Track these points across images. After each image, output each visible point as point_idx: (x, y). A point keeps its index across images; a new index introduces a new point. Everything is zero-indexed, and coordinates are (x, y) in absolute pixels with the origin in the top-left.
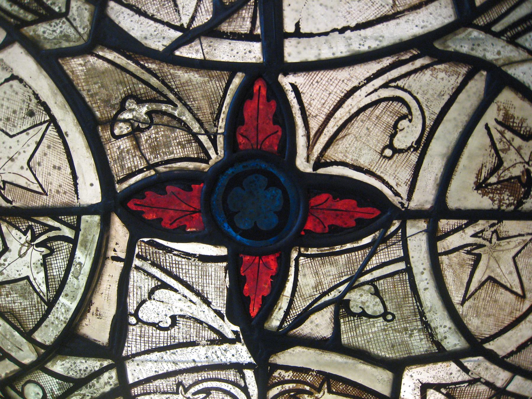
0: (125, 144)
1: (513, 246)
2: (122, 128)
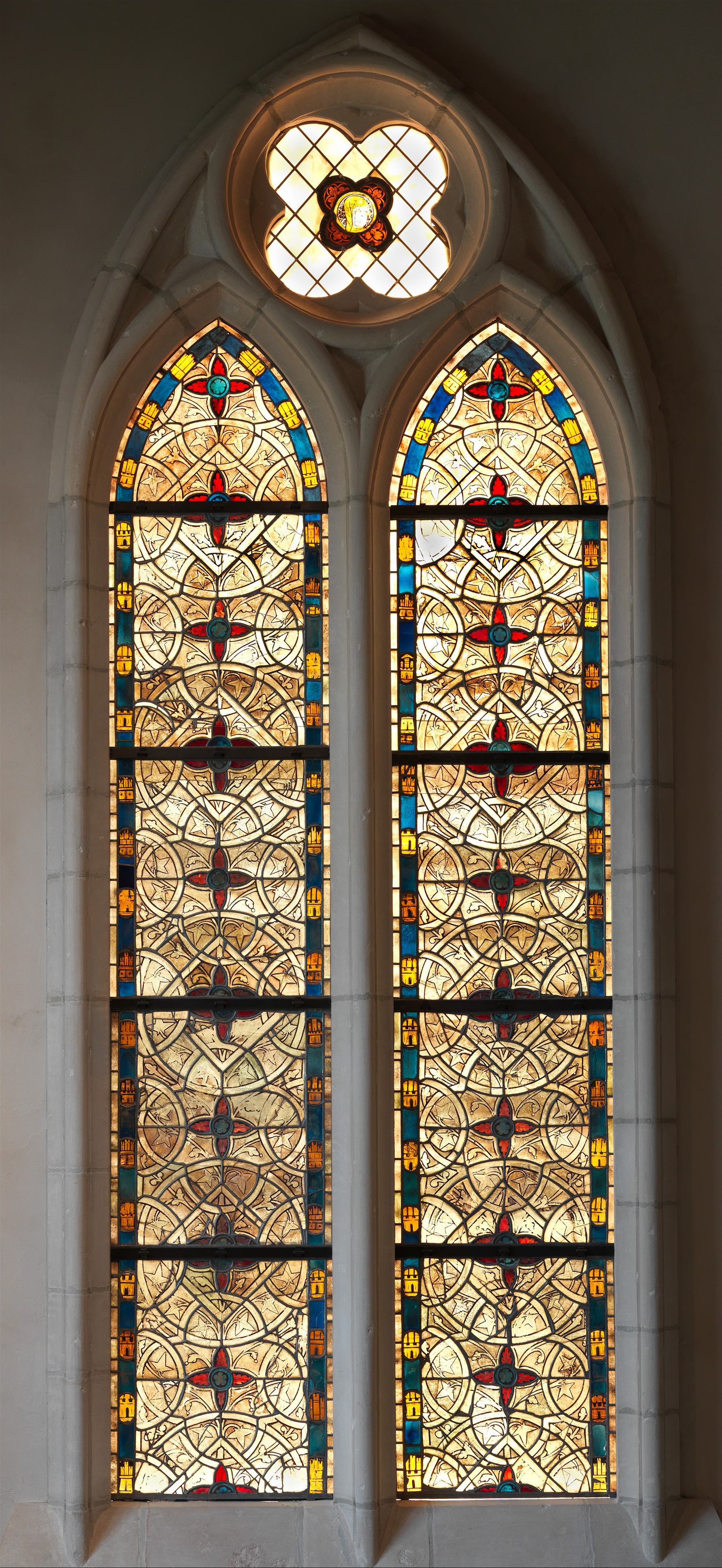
0: (475, 1362)
1: (569, 1386)
2: (474, 1358)
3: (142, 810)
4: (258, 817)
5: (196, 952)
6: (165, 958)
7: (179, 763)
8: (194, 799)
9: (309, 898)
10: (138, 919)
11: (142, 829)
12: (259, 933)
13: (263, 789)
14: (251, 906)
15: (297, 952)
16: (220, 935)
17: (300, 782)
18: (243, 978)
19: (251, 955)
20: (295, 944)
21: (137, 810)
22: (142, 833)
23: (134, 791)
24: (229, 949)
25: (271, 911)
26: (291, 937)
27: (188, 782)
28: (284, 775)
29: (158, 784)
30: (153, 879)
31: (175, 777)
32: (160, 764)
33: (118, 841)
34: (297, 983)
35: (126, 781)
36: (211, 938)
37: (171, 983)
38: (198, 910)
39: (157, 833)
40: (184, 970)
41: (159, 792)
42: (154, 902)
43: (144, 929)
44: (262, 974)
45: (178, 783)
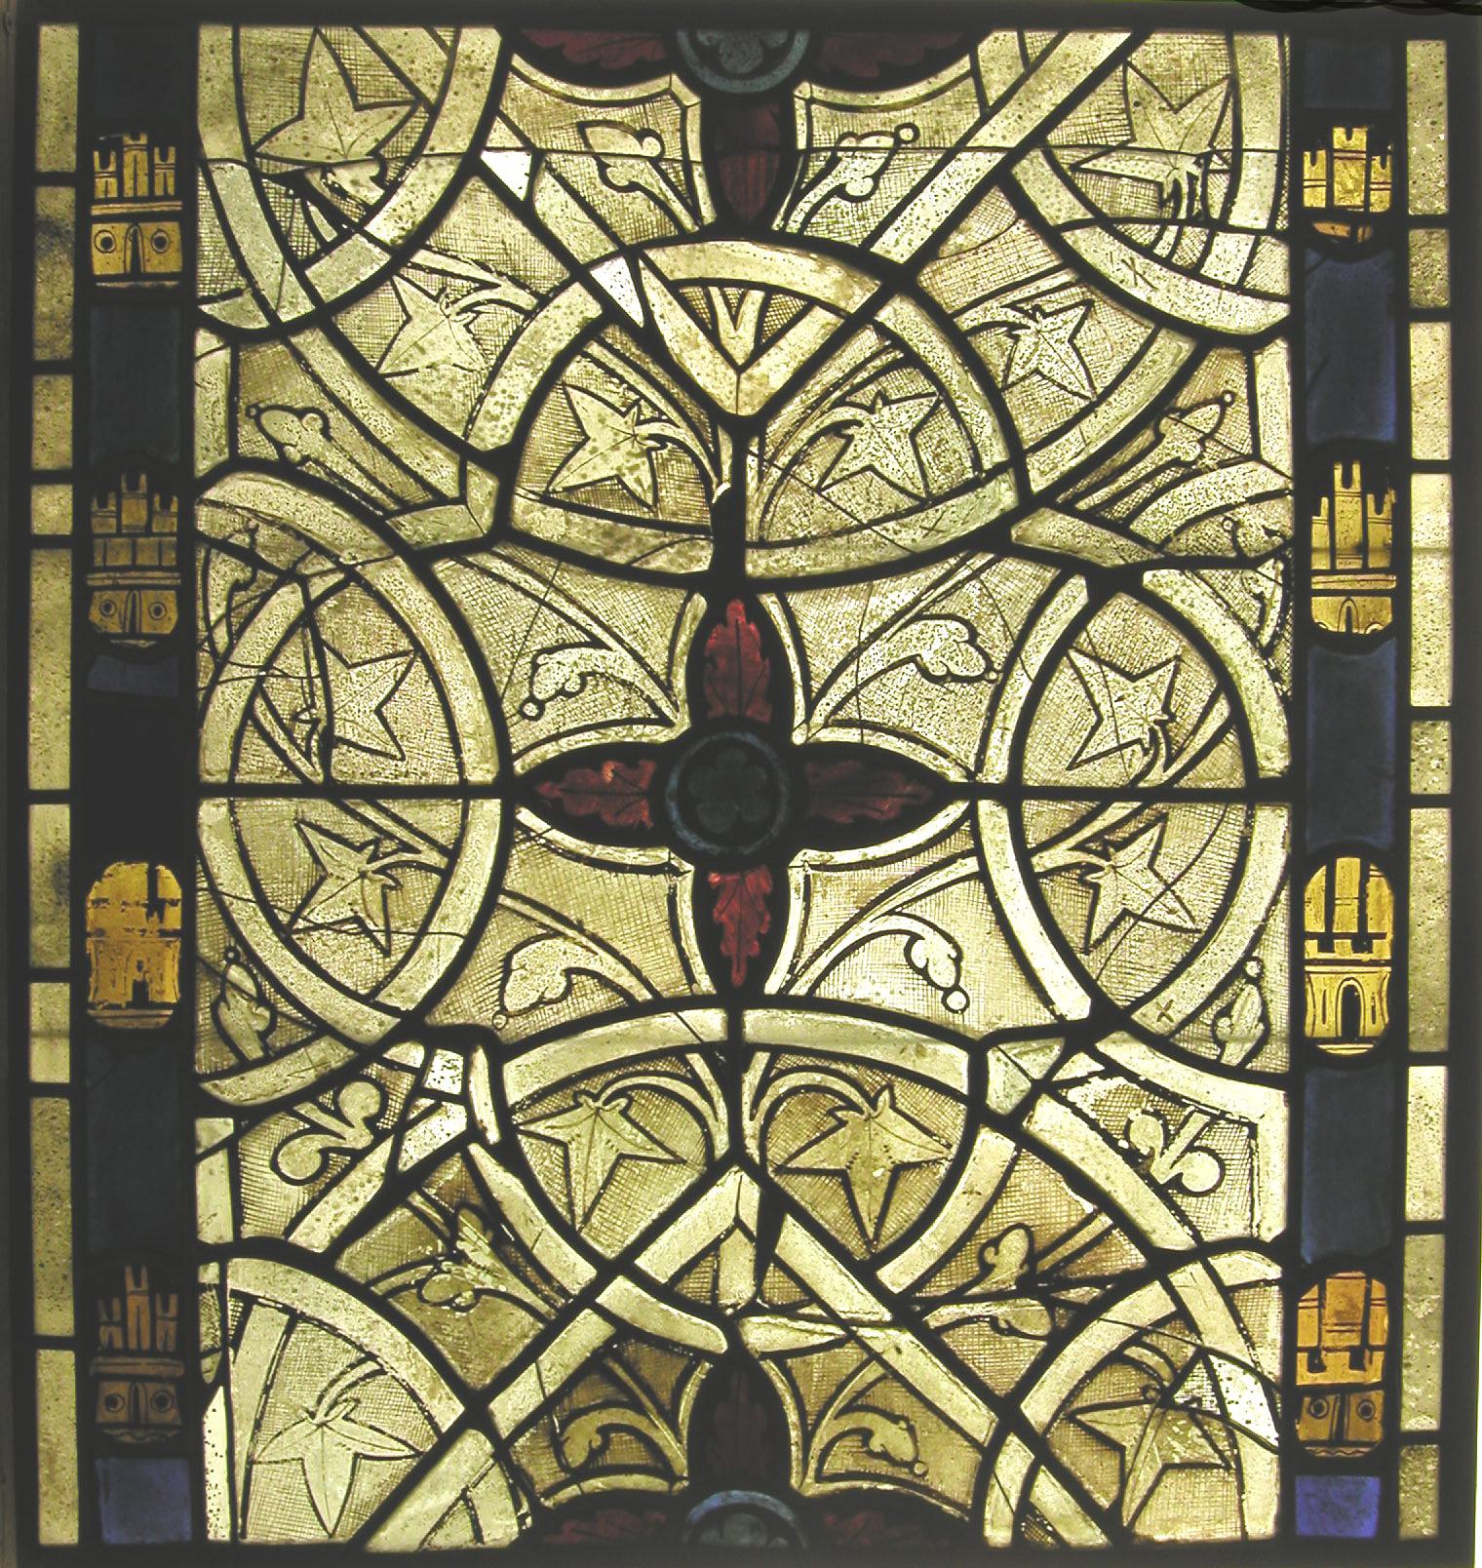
3: (235, 338)
4: (994, 396)
5: (587, 1272)
6: (382, 1306)
7: (482, 44)
8: (579, 272)
9: (1314, 923)
10: (207, 1057)
11: (237, 464)
12: (993, 1149)
13: (1026, 210)
14: (944, 975)
15: (1238, 1267)
16: (737, 1155)
17: (1259, 177)
18: (889, 1436)
19: (941, 1286)
20: (1222, 1220)
21: (204, 341)
22: (239, 489)
23: (188, 221)
24: (796, 1243)
25: (1075, 1005)
26: (1200, 1172)
27: (539, 159)
28: (1160, 129)
29: (343, 178)
30: (305, 789)
31: (453, 133)
32: (355, 50)
33: (80, 545)
34: (1234, 1466)
35: (135, 156)
36: (683, 1179)
37: (425, 1464)
38: (599, 1000)
39: (331, 489)
40: (506, 1378)
41: (348, 227)
42: (312, 945)
43: (250, 1117)
44: (1007, 1410)
45: (470, 166)
